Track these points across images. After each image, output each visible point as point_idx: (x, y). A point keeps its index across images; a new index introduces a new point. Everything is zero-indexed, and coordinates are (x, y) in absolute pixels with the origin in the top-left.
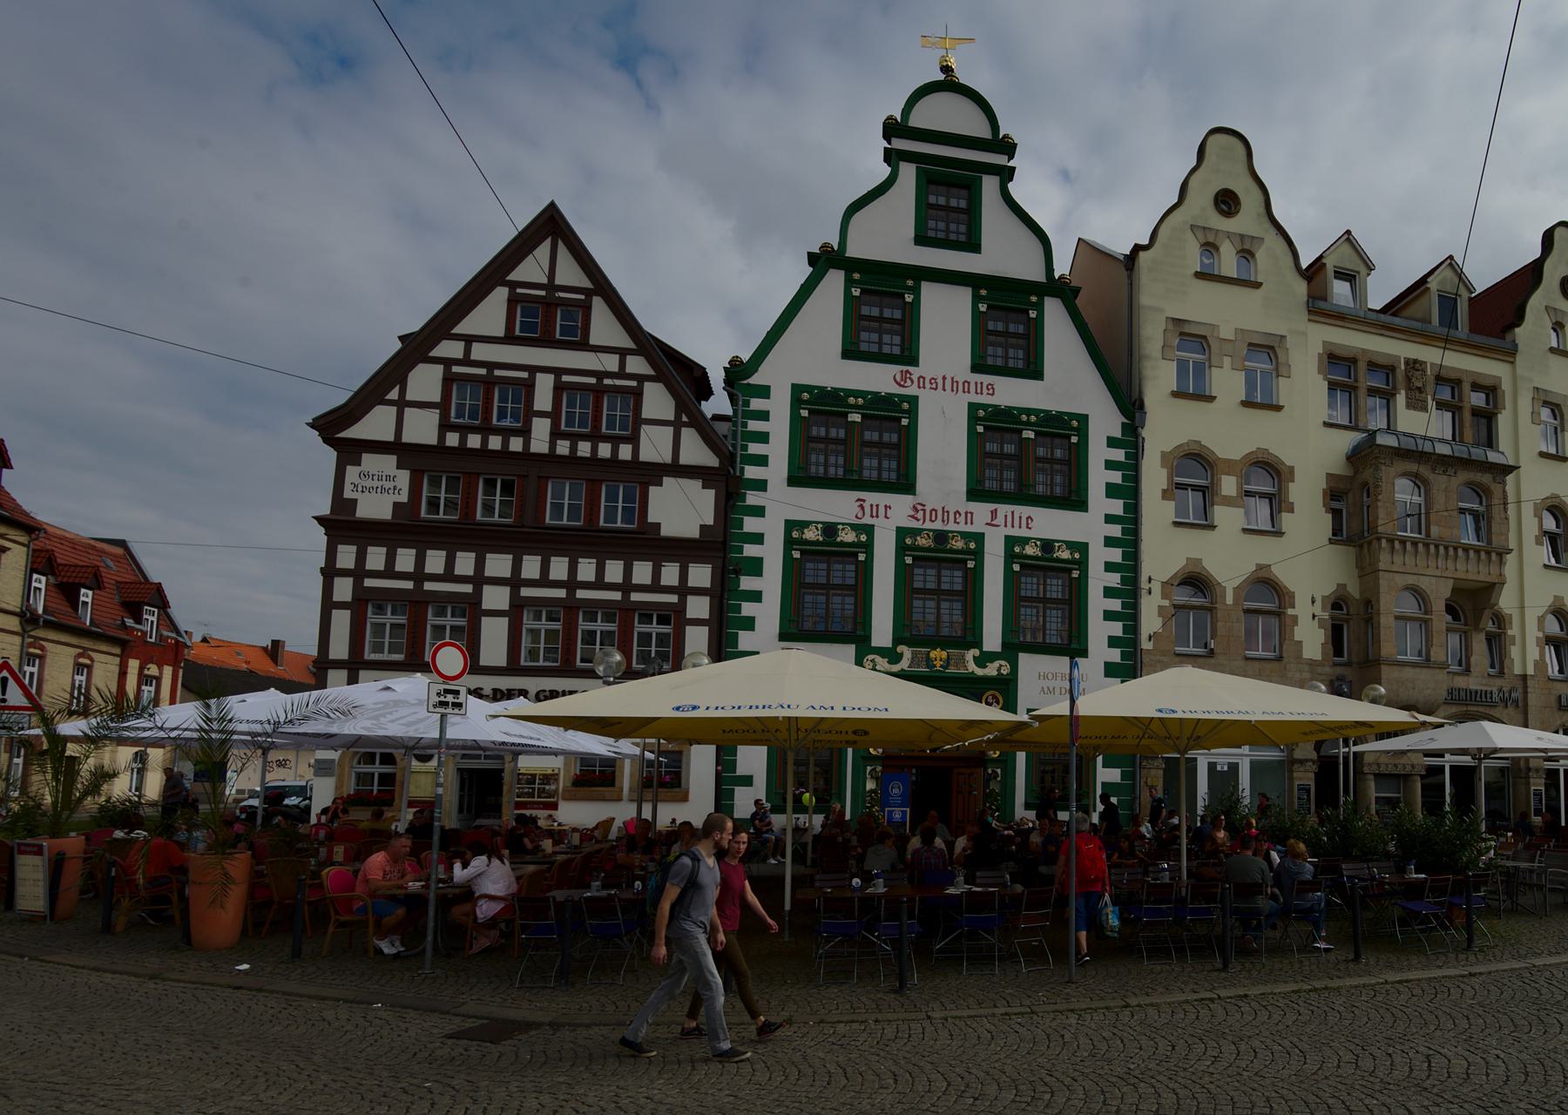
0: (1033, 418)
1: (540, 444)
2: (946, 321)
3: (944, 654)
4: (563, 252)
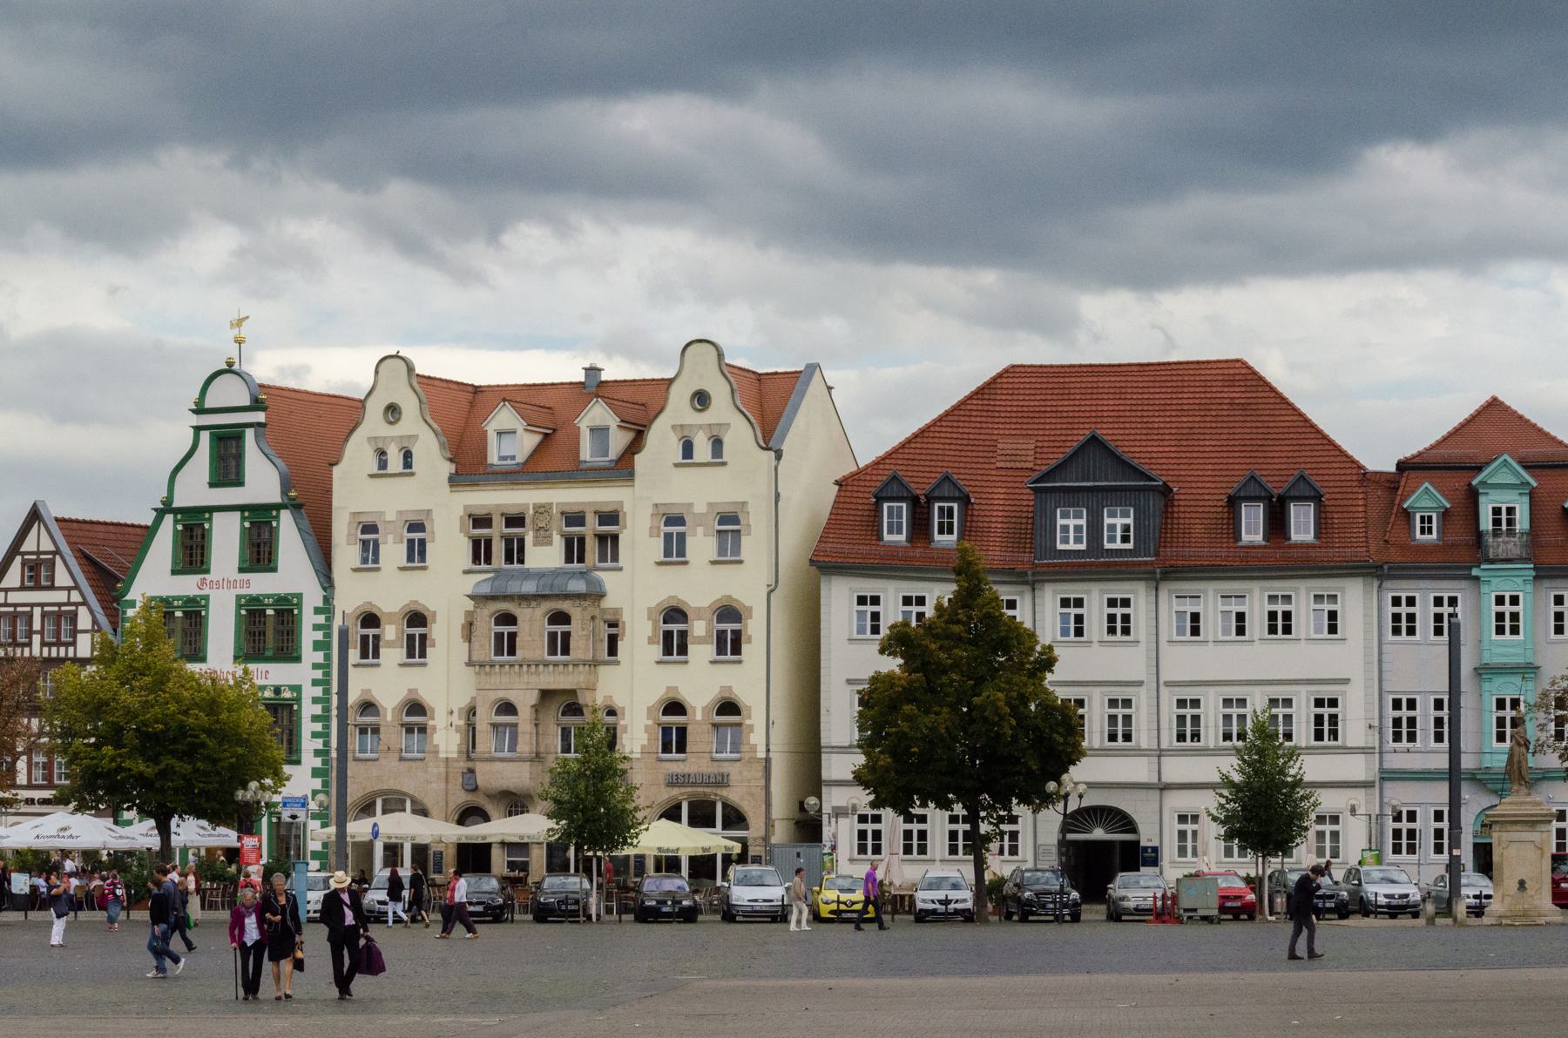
2: (226, 536)
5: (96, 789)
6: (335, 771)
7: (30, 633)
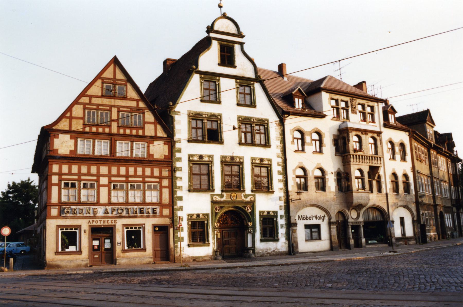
0: (255, 120)
3: (235, 195)
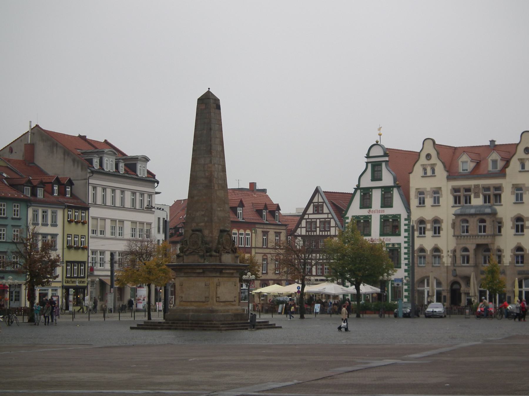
1: (318, 233)
2: (377, 197)
4: (320, 197)
5: (338, 275)
6: (411, 270)
7: (316, 228)
